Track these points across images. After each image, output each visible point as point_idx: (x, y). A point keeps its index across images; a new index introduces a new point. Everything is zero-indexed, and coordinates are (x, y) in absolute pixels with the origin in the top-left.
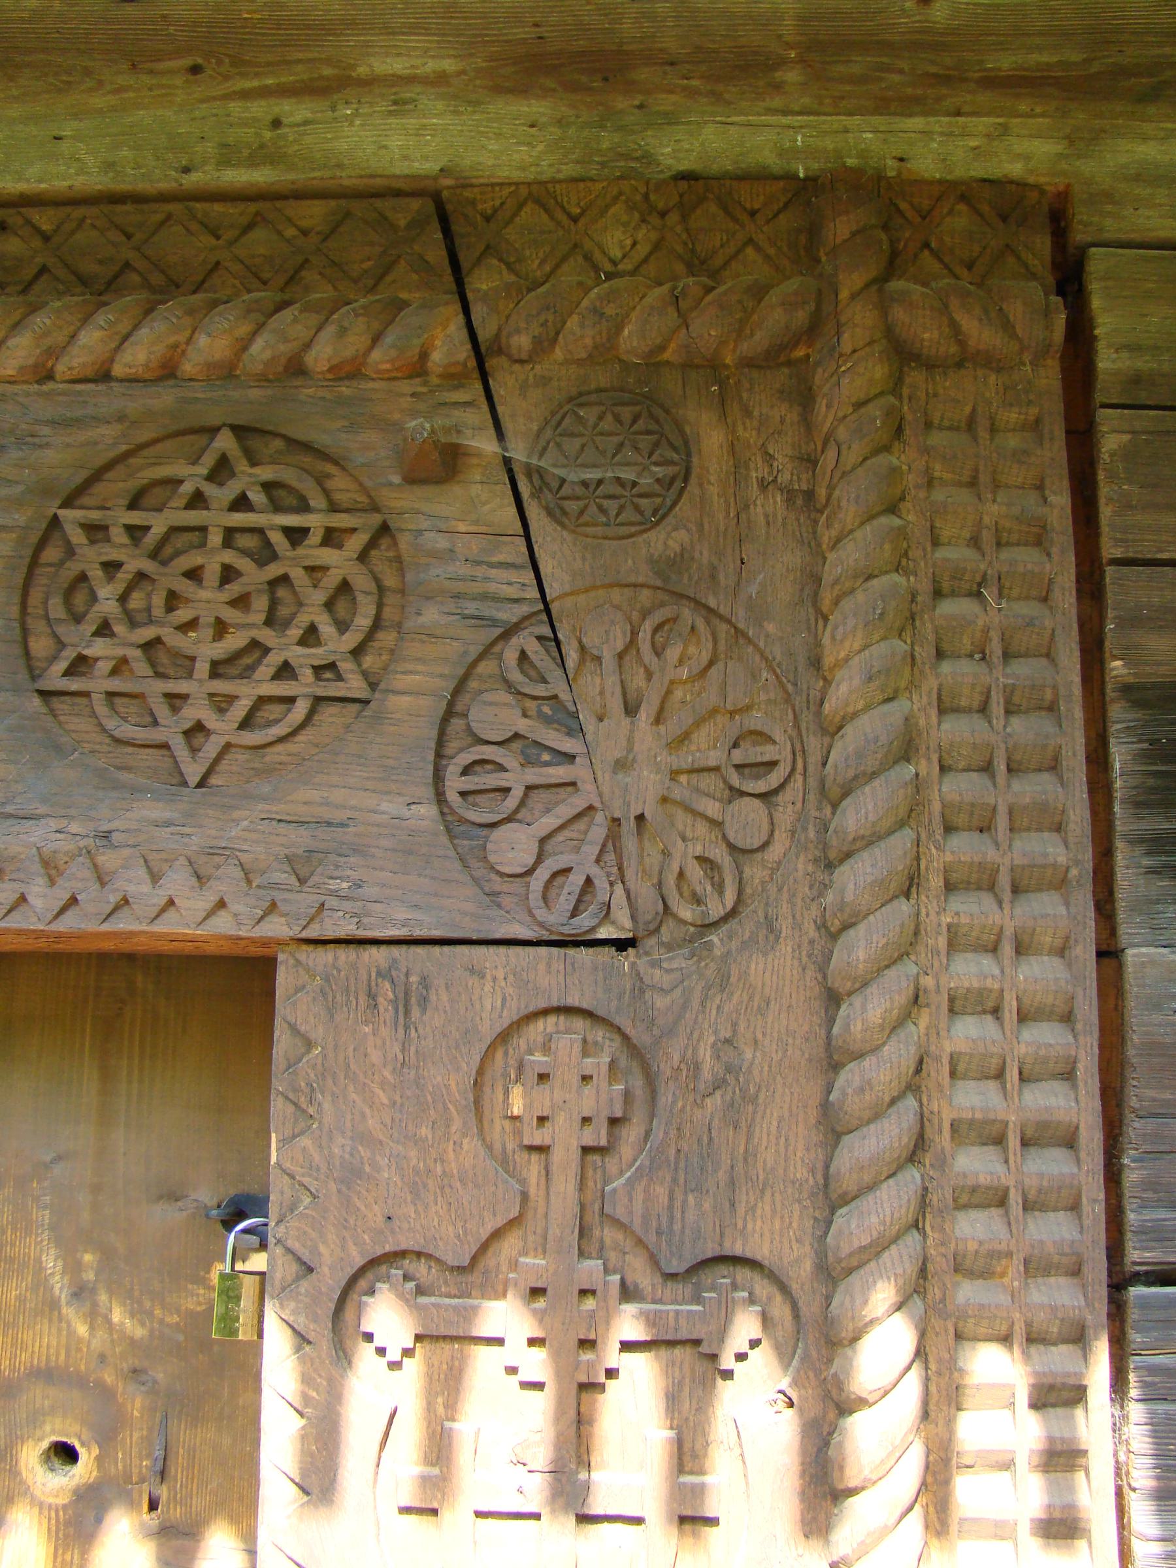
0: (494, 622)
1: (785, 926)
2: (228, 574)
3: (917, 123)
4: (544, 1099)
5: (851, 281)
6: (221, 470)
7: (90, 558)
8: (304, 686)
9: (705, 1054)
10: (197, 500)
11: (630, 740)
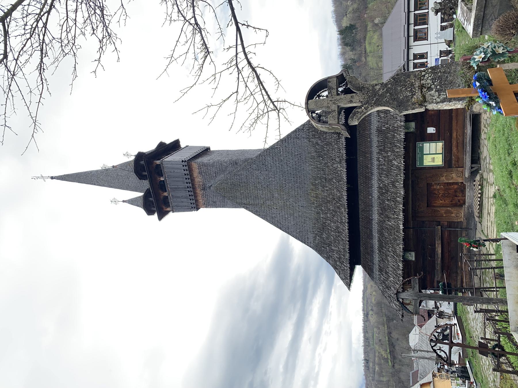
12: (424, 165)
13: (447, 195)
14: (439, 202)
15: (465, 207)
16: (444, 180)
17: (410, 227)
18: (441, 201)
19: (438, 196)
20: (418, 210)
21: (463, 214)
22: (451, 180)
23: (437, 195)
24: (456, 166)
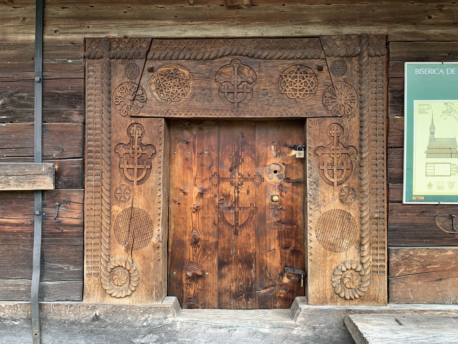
0: (327, 86)
1: (356, 115)
2: (300, 81)
3: (372, 27)
4: (333, 132)
5: (365, 48)
6: (299, 69)
7: (285, 79)
8: (309, 92)
9: (348, 127)
10: (296, 73)
11: (341, 97)
12: (417, 103)
13: (230, 218)
14: (190, 181)
15: (166, 310)
16: (319, 206)
17: (49, 28)
18: (196, 190)
19: (224, 179)
20: (151, 70)
21: (126, 302)
22: (320, 241)
23: (228, 174)
24: (398, 265)
